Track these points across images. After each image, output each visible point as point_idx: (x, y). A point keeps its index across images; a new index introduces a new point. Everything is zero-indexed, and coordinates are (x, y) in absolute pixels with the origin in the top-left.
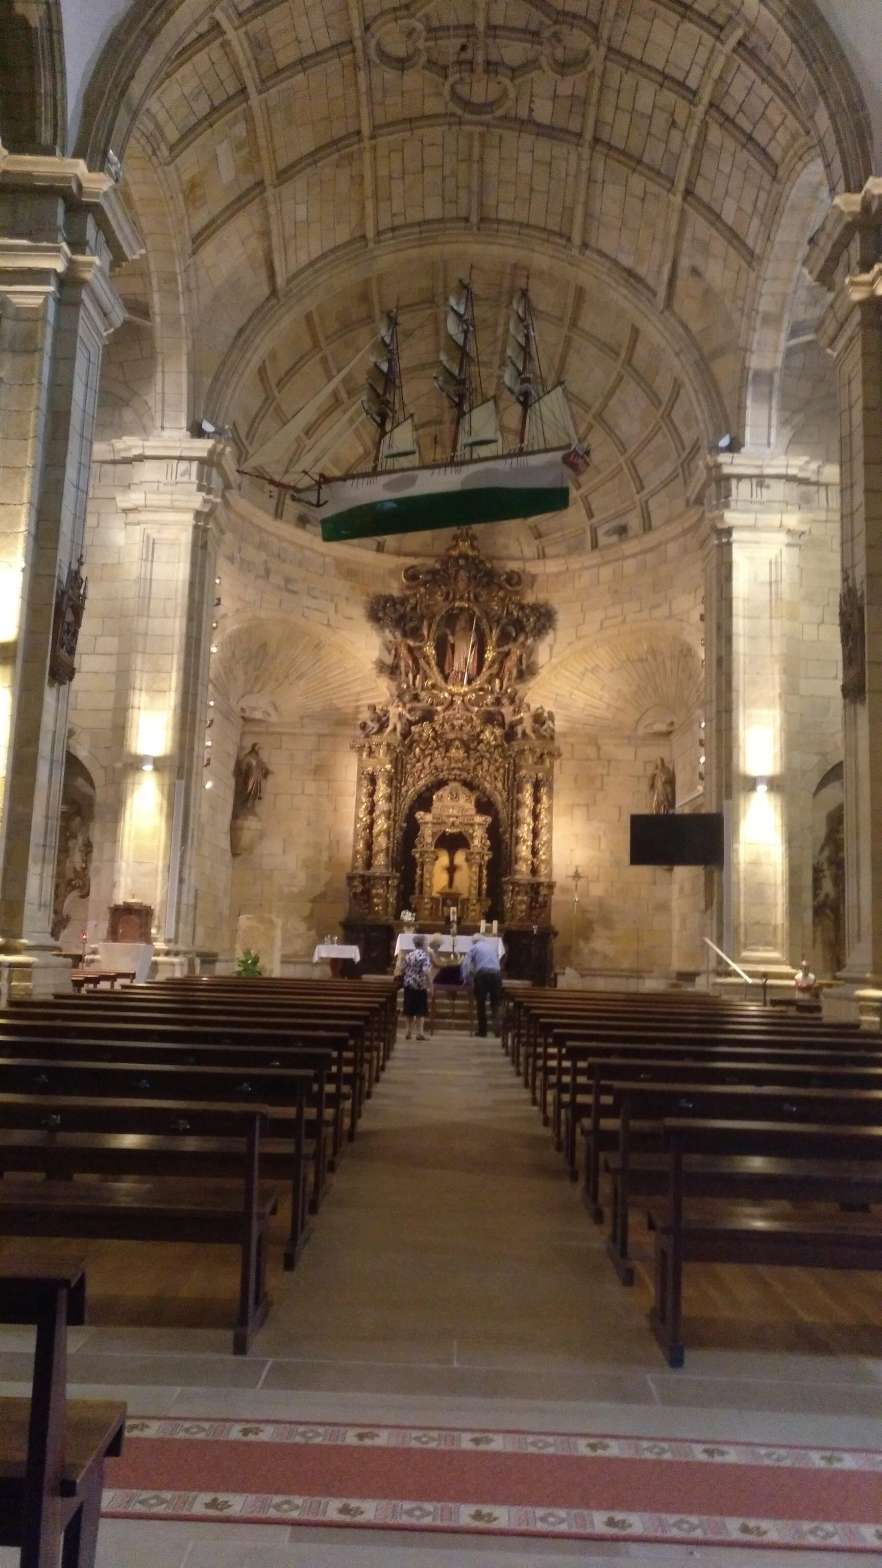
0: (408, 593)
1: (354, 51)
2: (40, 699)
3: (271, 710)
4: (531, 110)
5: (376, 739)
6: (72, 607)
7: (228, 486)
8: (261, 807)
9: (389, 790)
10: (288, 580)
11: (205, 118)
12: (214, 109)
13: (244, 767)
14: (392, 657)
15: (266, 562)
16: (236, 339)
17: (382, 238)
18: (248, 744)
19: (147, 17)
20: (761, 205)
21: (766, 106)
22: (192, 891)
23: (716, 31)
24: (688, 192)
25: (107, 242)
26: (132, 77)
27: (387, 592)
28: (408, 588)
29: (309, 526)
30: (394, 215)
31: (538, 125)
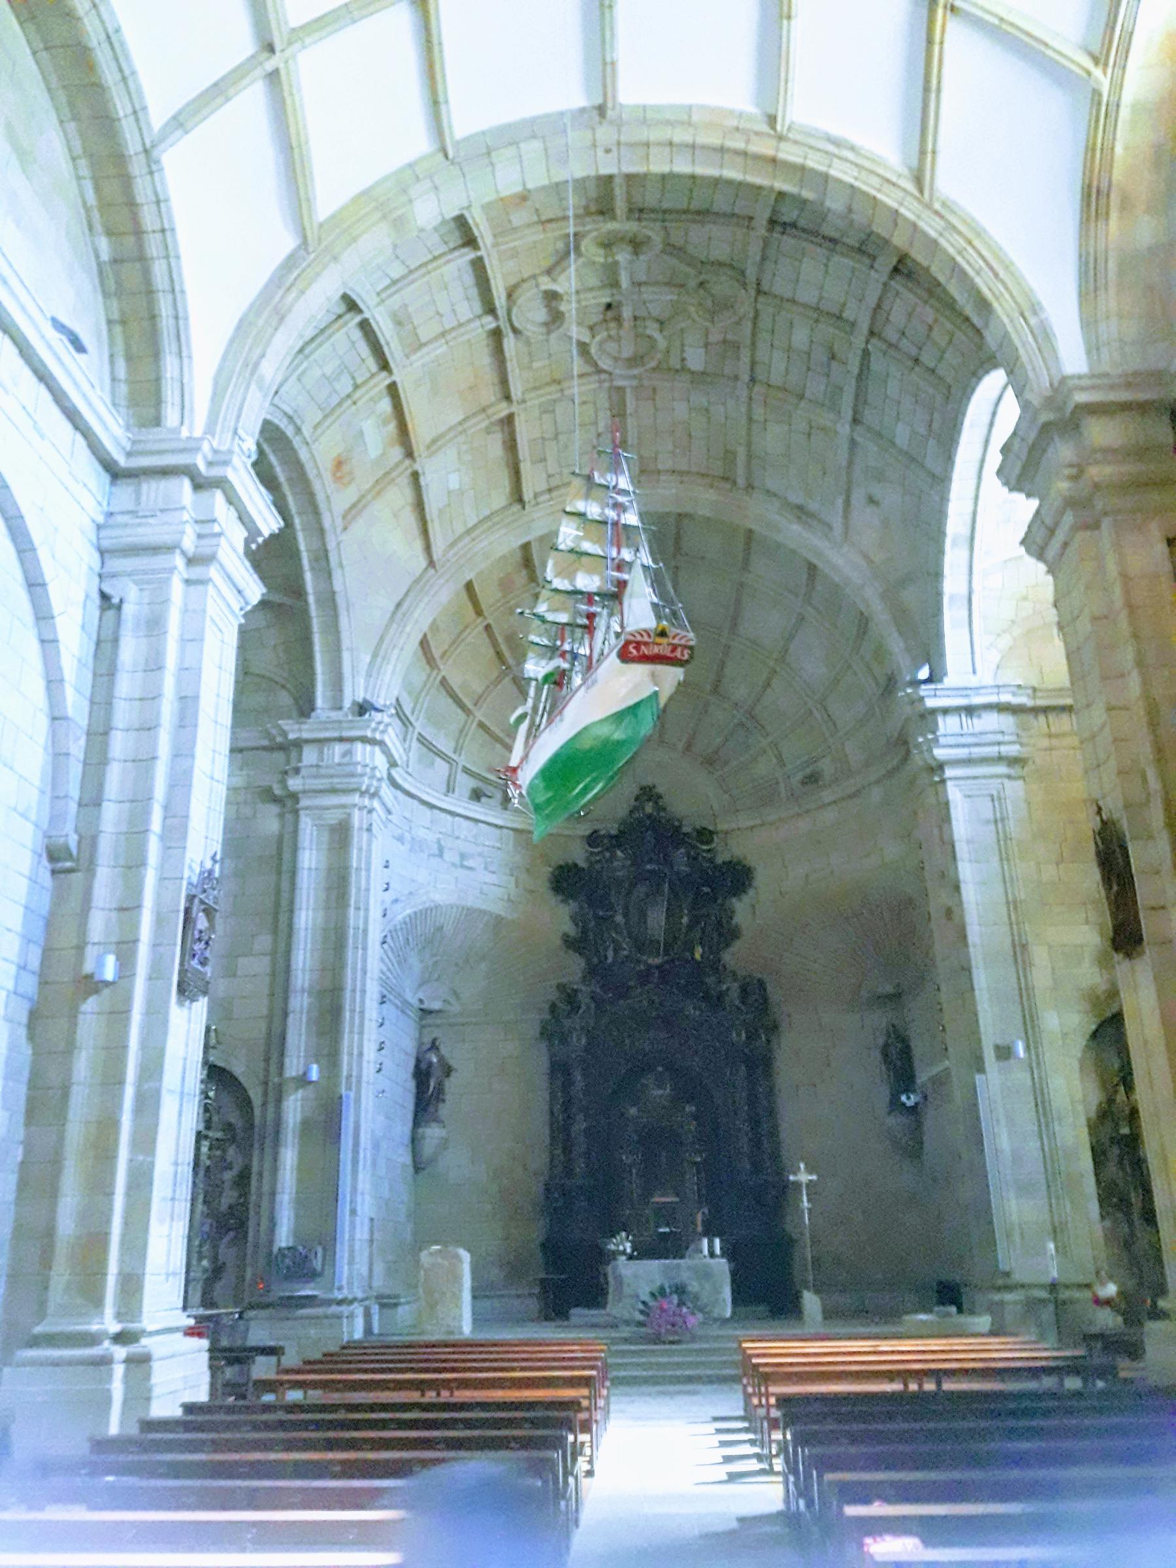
2: (165, 1023)
3: (452, 1000)
4: (683, 360)
5: (567, 1023)
6: (204, 910)
7: (393, 764)
8: (444, 1110)
10: (463, 856)
11: (349, 396)
12: (356, 387)
13: (423, 1066)
15: (439, 841)
16: (394, 613)
17: (541, 499)
18: (427, 1040)
19: (277, 298)
20: (936, 425)
21: (931, 328)
22: (367, 1221)
23: (867, 261)
24: (855, 421)
25: (240, 518)
26: (263, 356)
29: (483, 799)
30: (549, 476)
31: (693, 373)
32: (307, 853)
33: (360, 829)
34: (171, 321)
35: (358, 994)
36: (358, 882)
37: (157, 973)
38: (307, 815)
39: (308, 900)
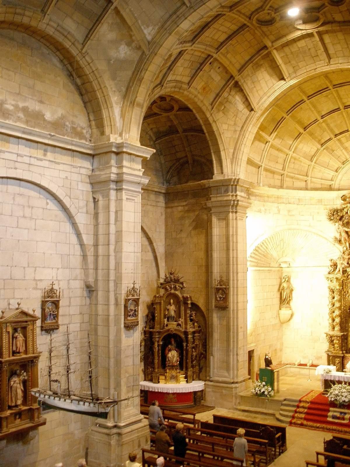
0: (344, 206)
1: (248, 26)
9: (339, 297)
14: (339, 236)
27: (335, 207)
28: (344, 204)
32: (215, 229)
33: (233, 219)
34: (103, 98)
35: (235, 281)
36: (233, 240)
37: (117, 322)
38: (214, 215)
39: (217, 247)
